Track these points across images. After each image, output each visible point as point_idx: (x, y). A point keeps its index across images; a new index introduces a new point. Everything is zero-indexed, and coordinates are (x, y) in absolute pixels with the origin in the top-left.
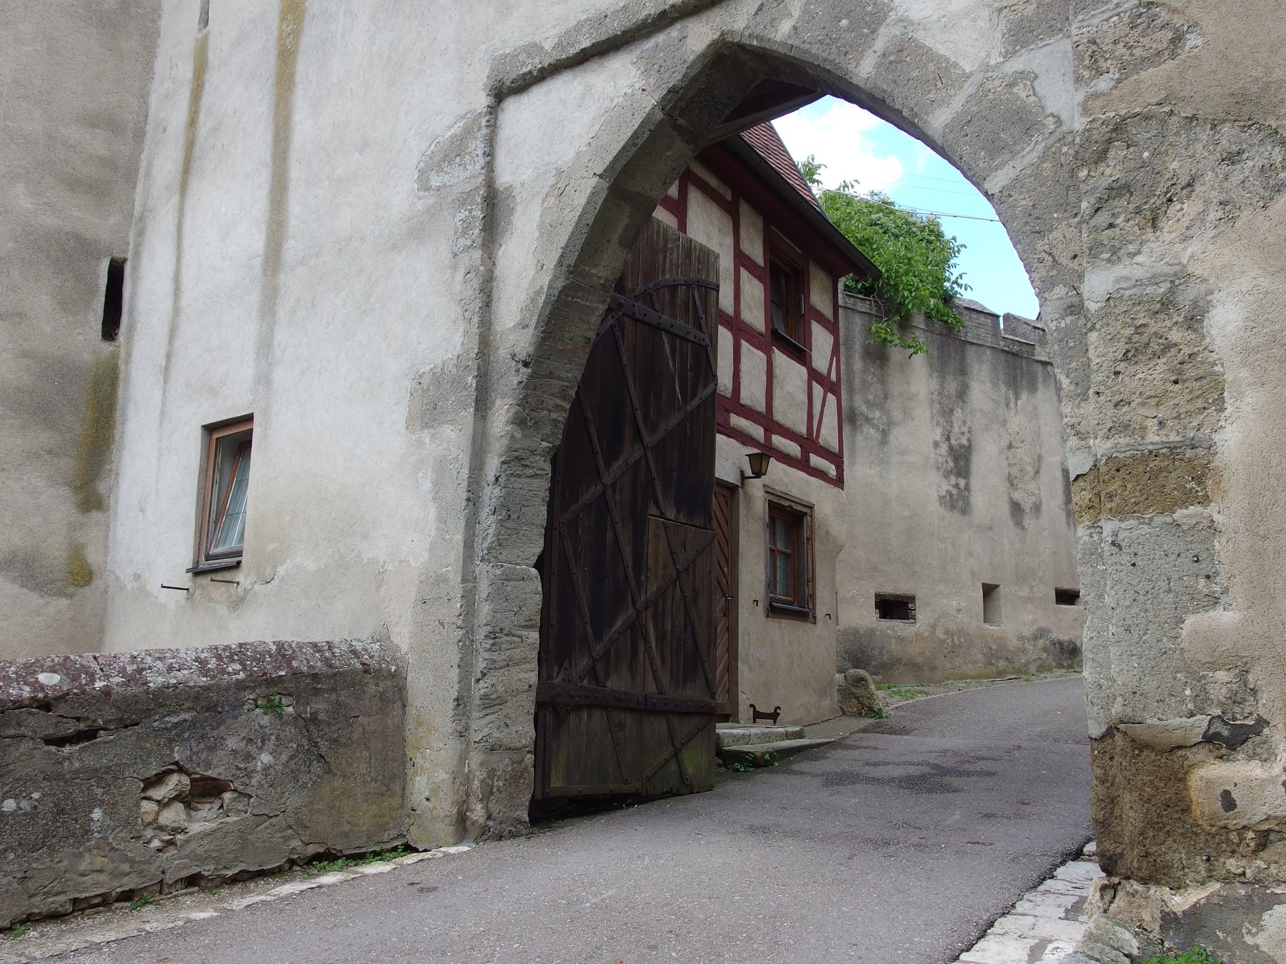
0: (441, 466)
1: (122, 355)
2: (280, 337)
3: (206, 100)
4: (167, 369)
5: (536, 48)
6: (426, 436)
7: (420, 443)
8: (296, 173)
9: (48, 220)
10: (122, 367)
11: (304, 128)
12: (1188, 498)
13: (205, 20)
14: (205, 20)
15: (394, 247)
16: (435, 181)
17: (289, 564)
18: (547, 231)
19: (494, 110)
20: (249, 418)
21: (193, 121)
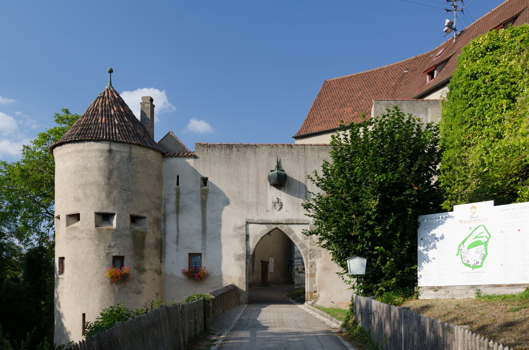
0: (241, 266)
1: (163, 237)
2: (207, 244)
3: (181, 199)
4: (177, 243)
5: (253, 220)
6: (238, 262)
7: (237, 262)
8: (208, 221)
9: (155, 216)
10: (163, 240)
11: (209, 214)
12: (314, 277)
13: (178, 184)
14: (178, 184)
15: (231, 237)
16: (237, 231)
17: (212, 274)
18: (254, 241)
19: (246, 225)
20: (201, 254)
21: (177, 202)
